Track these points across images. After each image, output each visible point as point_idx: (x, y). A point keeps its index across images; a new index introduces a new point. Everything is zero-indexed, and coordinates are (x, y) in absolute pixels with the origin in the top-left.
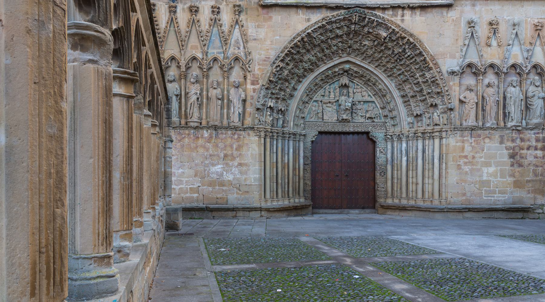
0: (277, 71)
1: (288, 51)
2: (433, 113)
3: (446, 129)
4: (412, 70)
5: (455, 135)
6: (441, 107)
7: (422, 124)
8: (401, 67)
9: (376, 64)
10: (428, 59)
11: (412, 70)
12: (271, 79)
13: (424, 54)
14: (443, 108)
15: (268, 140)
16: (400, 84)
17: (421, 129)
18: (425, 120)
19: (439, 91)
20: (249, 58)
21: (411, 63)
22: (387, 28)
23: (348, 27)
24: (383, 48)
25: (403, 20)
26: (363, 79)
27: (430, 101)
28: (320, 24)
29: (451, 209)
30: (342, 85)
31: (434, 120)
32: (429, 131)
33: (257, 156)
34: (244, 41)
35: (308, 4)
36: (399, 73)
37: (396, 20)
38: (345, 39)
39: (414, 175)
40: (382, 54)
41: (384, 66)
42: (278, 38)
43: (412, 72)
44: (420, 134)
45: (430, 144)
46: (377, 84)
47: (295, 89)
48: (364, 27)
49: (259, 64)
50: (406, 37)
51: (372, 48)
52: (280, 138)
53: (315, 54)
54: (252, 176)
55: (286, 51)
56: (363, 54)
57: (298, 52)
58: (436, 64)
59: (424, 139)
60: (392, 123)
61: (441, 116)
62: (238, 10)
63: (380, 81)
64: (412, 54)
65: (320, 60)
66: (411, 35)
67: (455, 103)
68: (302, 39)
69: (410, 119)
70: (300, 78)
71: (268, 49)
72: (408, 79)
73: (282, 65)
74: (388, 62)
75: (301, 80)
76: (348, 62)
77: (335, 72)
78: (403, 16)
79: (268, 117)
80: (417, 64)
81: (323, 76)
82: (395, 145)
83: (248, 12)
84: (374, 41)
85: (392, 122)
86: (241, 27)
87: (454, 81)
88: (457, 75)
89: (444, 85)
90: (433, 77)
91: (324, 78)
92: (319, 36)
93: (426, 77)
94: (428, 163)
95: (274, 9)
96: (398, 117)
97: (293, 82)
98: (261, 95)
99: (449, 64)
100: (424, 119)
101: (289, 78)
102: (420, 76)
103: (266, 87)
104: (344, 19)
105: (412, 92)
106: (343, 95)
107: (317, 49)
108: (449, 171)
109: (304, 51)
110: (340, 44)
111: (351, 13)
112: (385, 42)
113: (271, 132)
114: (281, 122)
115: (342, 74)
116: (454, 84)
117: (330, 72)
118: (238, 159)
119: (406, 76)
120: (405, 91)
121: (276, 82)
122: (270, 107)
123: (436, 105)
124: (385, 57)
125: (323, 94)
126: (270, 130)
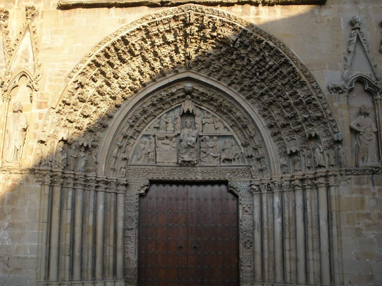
2: (314, 150)
3: (334, 173)
4: (278, 87)
6: (324, 139)
7: (301, 166)
8: (263, 84)
9: (229, 82)
10: (298, 70)
11: (278, 87)
12: (65, 99)
13: (292, 62)
14: (327, 141)
15: (57, 189)
16: (265, 109)
17: (299, 175)
18: (304, 161)
19: (319, 114)
20: (37, 72)
21: (276, 77)
24: (234, 57)
26: (214, 104)
27: (307, 131)
30: (183, 112)
31: (316, 159)
32: (311, 176)
33: (37, 214)
34: (34, 50)
36: (261, 91)
37: (248, 19)
39: (293, 247)
40: (234, 65)
41: (240, 83)
42: (80, 44)
43: (279, 91)
44: (297, 182)
45: (313, 197)
46: (234, 110)
49: (50, 81)
50: (262, 41)
51: (219, 59)
52: (80, 187)
54: (27, 244)
55: (89, 61)
56: (208, 67)
58: (309, 77)
59: (304, 189)
61: (325, 153)
62: (31, 13)
63: (237, 106)
64: (275, 64)
66: (270, 38)
67: (344, 133)
69: (283, 161)
72: (275, 101)
73: (81, 79)
74: (244, 77)
77: (173, 94)
78: (257, 14)
80: (285, 77)
82: (264, 200)
83: (44, 16)
84: (221, 48)
85: (260, 165)
86: (32, 33)
89: (325, 106)
90: (309, 96)
91: (155, 102)
93: (299, 96)
94: (312, 227)
95: (78, 10)
96: (266, 157)
98: (49, 122)
99: (327, 77)
100: (303, 159)
101: (97, 99)
102: (290, 95)
104: (175, 18)
105: (282, 119)
112: (236, 49)
113: (64, 178)
114: (82, 163)
115: (183, 97)
116: (340, 106)
117: (163, 93)
118: (9, 217)
119: (270, 96)
120: (274, 119)
123: (316, 137)
124: (240, 71)
126: (60, 174)
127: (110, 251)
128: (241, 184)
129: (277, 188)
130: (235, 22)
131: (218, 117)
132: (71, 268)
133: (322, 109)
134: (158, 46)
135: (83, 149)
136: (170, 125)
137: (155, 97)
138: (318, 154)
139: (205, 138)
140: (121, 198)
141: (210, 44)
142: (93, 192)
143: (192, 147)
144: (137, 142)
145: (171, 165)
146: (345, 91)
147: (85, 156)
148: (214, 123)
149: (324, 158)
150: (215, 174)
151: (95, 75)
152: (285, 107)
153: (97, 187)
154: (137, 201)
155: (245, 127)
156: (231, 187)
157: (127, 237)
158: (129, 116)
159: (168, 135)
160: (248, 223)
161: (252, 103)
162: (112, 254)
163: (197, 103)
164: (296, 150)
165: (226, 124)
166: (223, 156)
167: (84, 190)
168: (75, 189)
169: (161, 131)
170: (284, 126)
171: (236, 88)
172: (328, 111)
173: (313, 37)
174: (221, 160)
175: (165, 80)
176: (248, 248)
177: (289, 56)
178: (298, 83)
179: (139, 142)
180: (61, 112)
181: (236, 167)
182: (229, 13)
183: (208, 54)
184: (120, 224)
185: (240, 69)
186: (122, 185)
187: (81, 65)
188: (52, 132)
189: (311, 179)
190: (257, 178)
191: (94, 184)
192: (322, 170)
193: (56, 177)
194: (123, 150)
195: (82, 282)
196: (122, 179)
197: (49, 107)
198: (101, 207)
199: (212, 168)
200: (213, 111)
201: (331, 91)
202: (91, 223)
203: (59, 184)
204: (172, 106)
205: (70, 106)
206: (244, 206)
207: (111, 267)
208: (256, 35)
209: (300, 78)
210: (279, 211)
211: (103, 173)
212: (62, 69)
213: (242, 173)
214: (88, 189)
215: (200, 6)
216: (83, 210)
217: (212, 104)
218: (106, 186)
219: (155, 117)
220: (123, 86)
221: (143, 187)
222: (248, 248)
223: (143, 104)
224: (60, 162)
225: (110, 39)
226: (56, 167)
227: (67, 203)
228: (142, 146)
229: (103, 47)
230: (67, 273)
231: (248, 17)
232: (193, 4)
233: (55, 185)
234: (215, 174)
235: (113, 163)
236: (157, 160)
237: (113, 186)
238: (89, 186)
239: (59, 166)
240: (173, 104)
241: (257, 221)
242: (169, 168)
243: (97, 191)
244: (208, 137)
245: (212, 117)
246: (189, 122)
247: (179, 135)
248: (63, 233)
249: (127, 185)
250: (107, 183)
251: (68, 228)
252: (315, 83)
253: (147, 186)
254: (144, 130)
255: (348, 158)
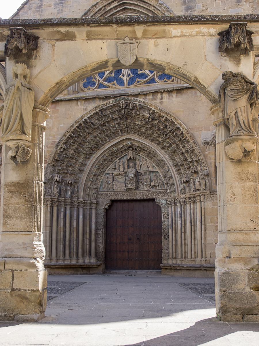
0: (63, 152)
1: (69, 135)
3: (203, 194)
5: (212, 198)
6: (201, 174)
7: (190, 189)
10: (184, 133)
12: (56, 158)
13: (181, 128)
15: (55, 208)
19: (196, 159)
22: (149, 110)
23: (119, 112)
25: (161, 103)
28: (94, 112)
29: (206, 267)
35: (84, 97)
38: (119, 121)
42: (62, 125)
44: (187, 199)
47: (83, 165)
48: (132, 110)
50: (164, 116)
52: (68, 206)
53: (98, 135)
55: (68, 136)
57: (79, 135)
60: (172, 190)
64: (172, 129)
65: (103, 139)
66: (168, 114)
68: (80, 124)
70: (88, 156)
71: (55, 135)
75: (88, 157)
76: (128, 139)
78: (162, 99)
79: (55, 189)
80: (179, 137)
81: (110, 153)
87: (209, 150)
88: (211, 145)
91: (111, 154)
92: (97, 121)
97: (81, 160)
103: (52, 165)
106: (130, 167)
107: (98, 132)
108: (207, 232)
109: (85, 134)
110: (117, 126)
111: (118, 101)
114: (69, 193)
116: (210, 153)
117: (115, 149)
121: (63, 160)
122: (56, 181)
125: (114, 167)
127: (87, 242)
128: (161, 200)
129: (178, 203)
130: (148, 105)
131: (149, 160)
132: (64, 251)
133: (199, 156)
134: (107, 122)
135: (69, 185)
136: (121, 167)
137: (110, 151)
138: (197, 183)
139: (142, 173)
140: (94, 211)
141: (137, 118)
142: (76, 209)
143: (132, 180)
144: (102, 178)
145: (122, 190)
146: (213, 144)
147: (70, 189)
148: (147, 164)
149: (200, 185)
150: (147, 195)
151: (72, 142)
152: (181, 154)
153: (79, 205)
154: (103, 212)
155: (163, 166)
156: (157, 202)
157: (98, 233)
158: (96, 164)
159: (120, 173)
160: (166, 224)
161: (165, 152)
162: (88, 243)
163: (136, 153)
164: (187, 180)
165: (154, 164)
166: (152, 184)
167: (71, 208)
168: (66, 207)
169: (116, 170)
170: (183, 165)
171: (156, 143)
172: (201, 157)
173: (195, 111)
174: (151, 186)
175: (115, 141)
176: (167, 239)
177: (179, 125)
178: (185, 140)
179: (104, 178)
180: (55, 165)
181: (160, 190)
182: (144, 100)
183: (137, 124)
184: (93, 226)
185: (155, 132)
186: (93, 204)
187: (64, 138)
188: (50, 177)
189: (194, 197)
190: (170, 197)
191: (76, 204)
192: (198, 192)
193: (54, 202)
194: (94, 183)
195: (70, 259)
196: (94, 200)
197: (48, 163)
198: (81, 217)
199: (145, 191)
200: (146, 157)
201: (204, 145)
202: (75, 225)
203: (55, 206)
204: (122, 155)
205: (60, 162)
206: (164, 214)
207: (88, 251)
208: (160, 113)
209: (186, 138)
210: (180, 216)
211: (82, 198)
212: (54, 141)
213: (163, 194)
214: (73, 207)
215: (127, 97)
216: (70, 219)
217: (145, 153)
218: (84, 205)
219: (112, 162)
220: (90, 147)
221: (107, 204)
222: (167, 239)
223: (104, 155)
224: (56, 193)
225: (78, 122)
226: (54, 196)
227: (61, 215)
228: (105, 180)
229: (75, 127)
230: (62, 253)
231: (156, 101)
232: (124, 97)
233: (54, 206)
234: (147, 195)
235: (88, 191)
236: (114, 188)
237: (88, 204)
238: (73, 205)
239: (55, 196)
240: (122, 154)
241: (170, 223)
242: (120, 192)
243: (79, 208)
244: (143, 173)
245: (146, 160)
246: (131, 164)
247: (126, 172)
248: (59, 232)
249: (97, 204)
250: (84, 203)
251: (62, 229)
252: (193, 141)
253: (109, 203)
254: (107, 170)
255: (213, 184)
